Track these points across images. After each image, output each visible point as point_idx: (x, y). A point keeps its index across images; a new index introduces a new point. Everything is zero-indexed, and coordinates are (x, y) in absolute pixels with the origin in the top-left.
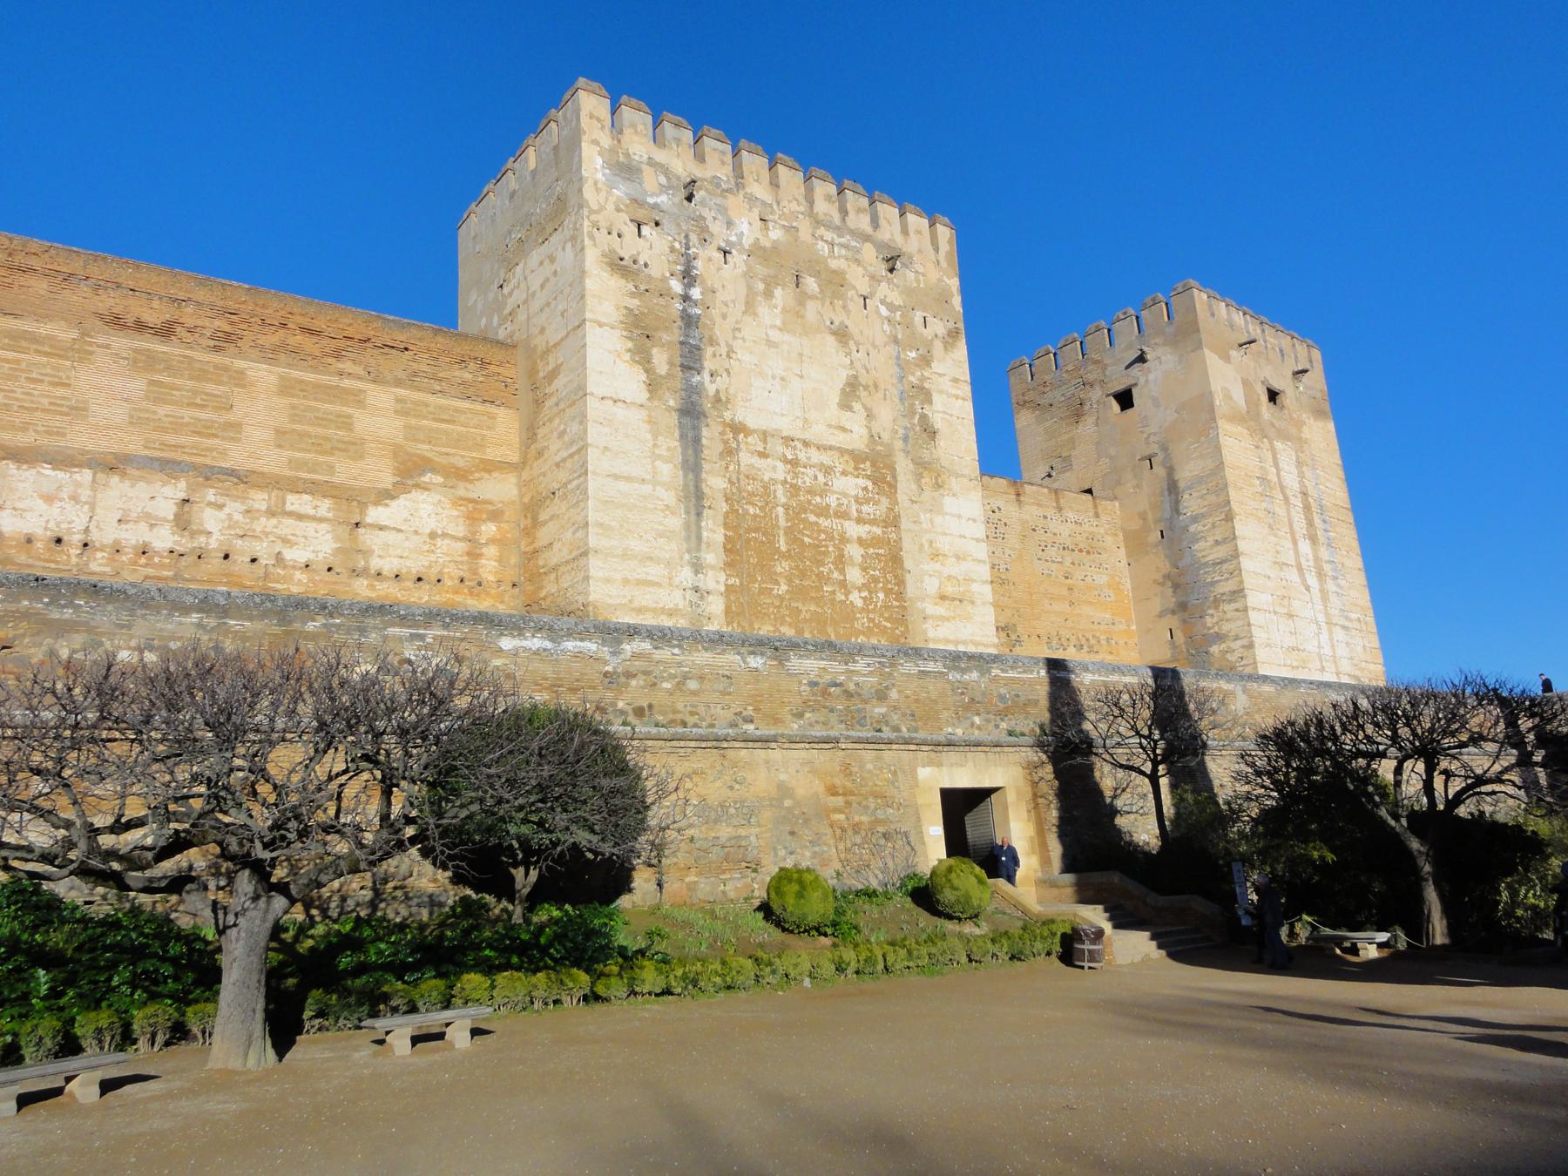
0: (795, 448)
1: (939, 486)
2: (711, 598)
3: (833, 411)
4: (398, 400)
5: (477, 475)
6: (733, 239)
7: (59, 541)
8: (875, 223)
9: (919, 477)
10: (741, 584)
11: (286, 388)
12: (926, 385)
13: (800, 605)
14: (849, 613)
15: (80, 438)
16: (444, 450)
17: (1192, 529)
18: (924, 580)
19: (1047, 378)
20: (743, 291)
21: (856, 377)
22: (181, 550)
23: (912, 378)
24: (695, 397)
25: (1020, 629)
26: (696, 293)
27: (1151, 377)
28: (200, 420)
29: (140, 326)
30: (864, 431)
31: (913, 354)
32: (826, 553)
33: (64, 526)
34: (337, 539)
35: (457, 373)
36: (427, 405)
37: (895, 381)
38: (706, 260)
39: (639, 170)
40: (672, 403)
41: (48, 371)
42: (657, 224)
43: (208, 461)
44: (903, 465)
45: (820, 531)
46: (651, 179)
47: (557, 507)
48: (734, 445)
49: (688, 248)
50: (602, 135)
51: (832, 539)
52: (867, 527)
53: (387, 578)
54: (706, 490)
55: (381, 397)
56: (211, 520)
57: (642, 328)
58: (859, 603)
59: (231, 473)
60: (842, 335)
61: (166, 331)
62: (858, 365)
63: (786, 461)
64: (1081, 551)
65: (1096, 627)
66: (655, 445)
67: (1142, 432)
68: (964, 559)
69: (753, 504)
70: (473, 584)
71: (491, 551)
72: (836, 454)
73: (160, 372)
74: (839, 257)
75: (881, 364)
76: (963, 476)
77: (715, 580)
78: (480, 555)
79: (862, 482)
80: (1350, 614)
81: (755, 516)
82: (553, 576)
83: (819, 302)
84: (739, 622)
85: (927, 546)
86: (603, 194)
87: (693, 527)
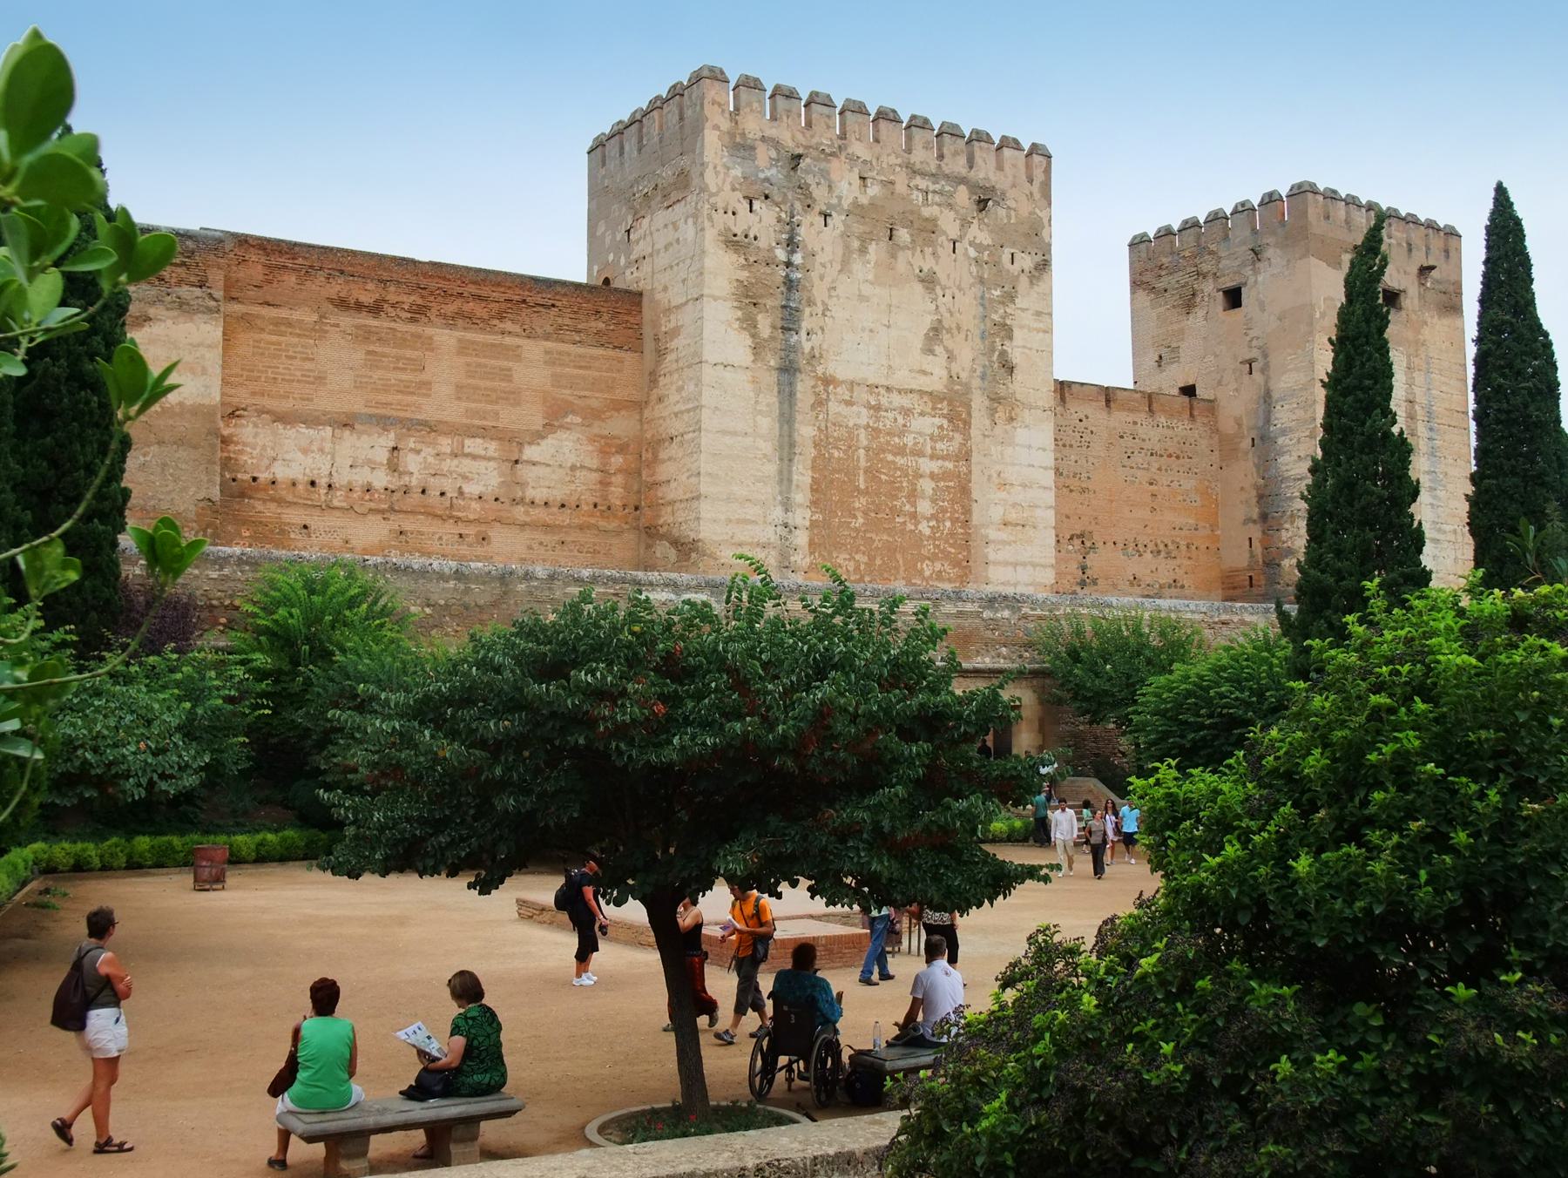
0: (878, 394)
1: (1012, 419)
2: (797, 532)
3: (917, 358)
4: (547, 352)
5: (608, 414)
6: (834, 201)
7: (313, 483)
8: (971, 164)
9: (992, 412)
10: (824, 519)
11: (463, 348)
12: (1008, 322)
13: (874, 536)
14: (918, 539)
15: (324, 403)
16: (582, 393)
17: (1280, 441)
18: (989, 507)
19: (1164, 260)
20: (840, 251)
21: (940, 321)
22: (391, 487)
23: (995, 317)
24: (792, 356)
25: (1096, 537)
26: (797, 259)
27: (1260, 278)
28: (402, 381)
29: (359, 306)
30: (944, 373)
31: (997, 293)
32: (900, 489)
33: (315, 472)
34: (501, 474)
35: (593, 324)
36: (569, 355)
37: (976, 321)
38: (810, 230)
39: (753, 148)
40: (772, 363)
41: (299, 349)
42: (767, 197)
43: (408, 415)
44: (979, 402)
45: (897, 469)
46: (764, 154)
47: (673, 450)
48: (824, 397)
49: (792, 217)
50: (722, 119)
51: (907, 475)
52: (940, 462)
53: (539, 506)
54: (797, 437)
55: (534, 350)
56: (412, 462)
57: (751, 297)
58: (927, 532)
59: (424, 423)
60: (929, 281)
61: (376, 309)
62: (942, 309)
63: (870, 407)
64: (1170, 456)
65: (1177, 532)
66: (757, 402)
67: (1246, 334)
68: (1031, 487)
69: (839, 449)
70: (604, 508)
71: (618, 479)
72: (915, 396)
73: (374, 343)
74: (932, 205)
75: (966, 308)
76: (1037, 407)
77: (802, 517)
78: (609, 484)
79: (937, 421)
80: (1444, 527)
81: (839, 459)
82: (669, 509)
83: (910, 253)
84: (820, 555)
85: (995, 475)
86: (722, 176)
87: (785, 473)
